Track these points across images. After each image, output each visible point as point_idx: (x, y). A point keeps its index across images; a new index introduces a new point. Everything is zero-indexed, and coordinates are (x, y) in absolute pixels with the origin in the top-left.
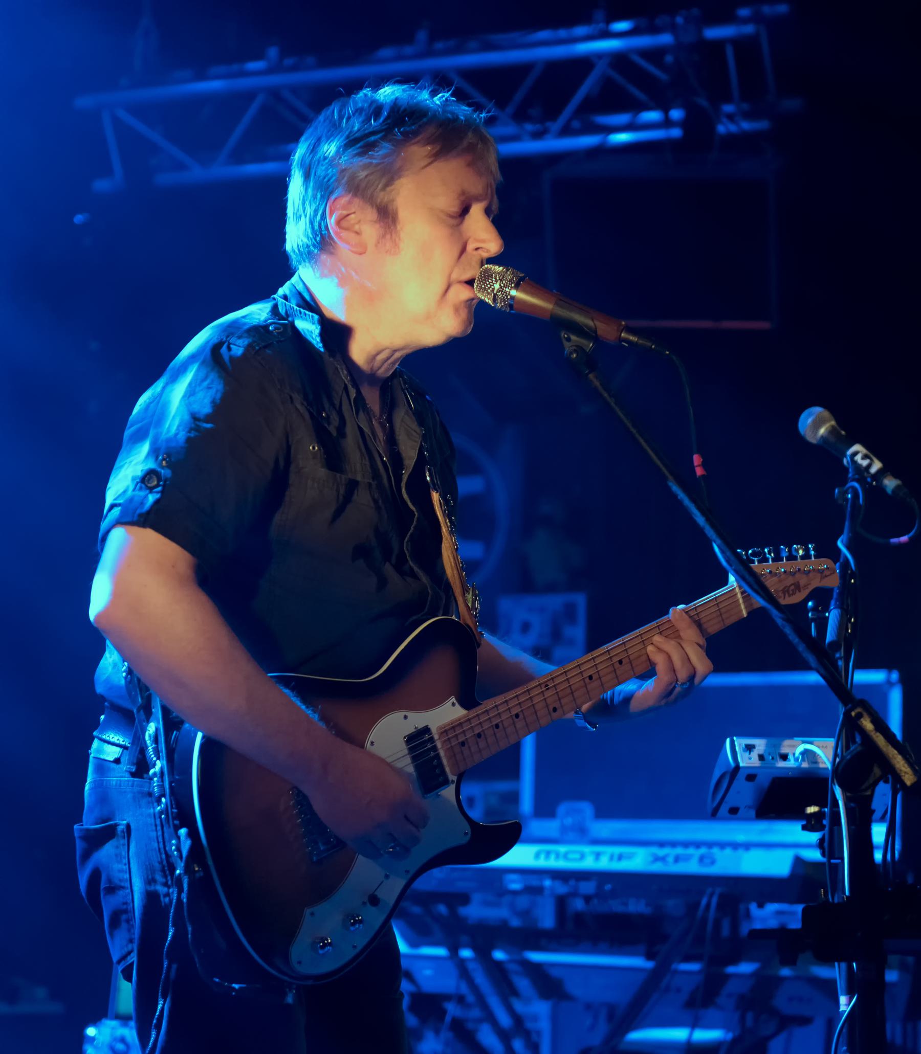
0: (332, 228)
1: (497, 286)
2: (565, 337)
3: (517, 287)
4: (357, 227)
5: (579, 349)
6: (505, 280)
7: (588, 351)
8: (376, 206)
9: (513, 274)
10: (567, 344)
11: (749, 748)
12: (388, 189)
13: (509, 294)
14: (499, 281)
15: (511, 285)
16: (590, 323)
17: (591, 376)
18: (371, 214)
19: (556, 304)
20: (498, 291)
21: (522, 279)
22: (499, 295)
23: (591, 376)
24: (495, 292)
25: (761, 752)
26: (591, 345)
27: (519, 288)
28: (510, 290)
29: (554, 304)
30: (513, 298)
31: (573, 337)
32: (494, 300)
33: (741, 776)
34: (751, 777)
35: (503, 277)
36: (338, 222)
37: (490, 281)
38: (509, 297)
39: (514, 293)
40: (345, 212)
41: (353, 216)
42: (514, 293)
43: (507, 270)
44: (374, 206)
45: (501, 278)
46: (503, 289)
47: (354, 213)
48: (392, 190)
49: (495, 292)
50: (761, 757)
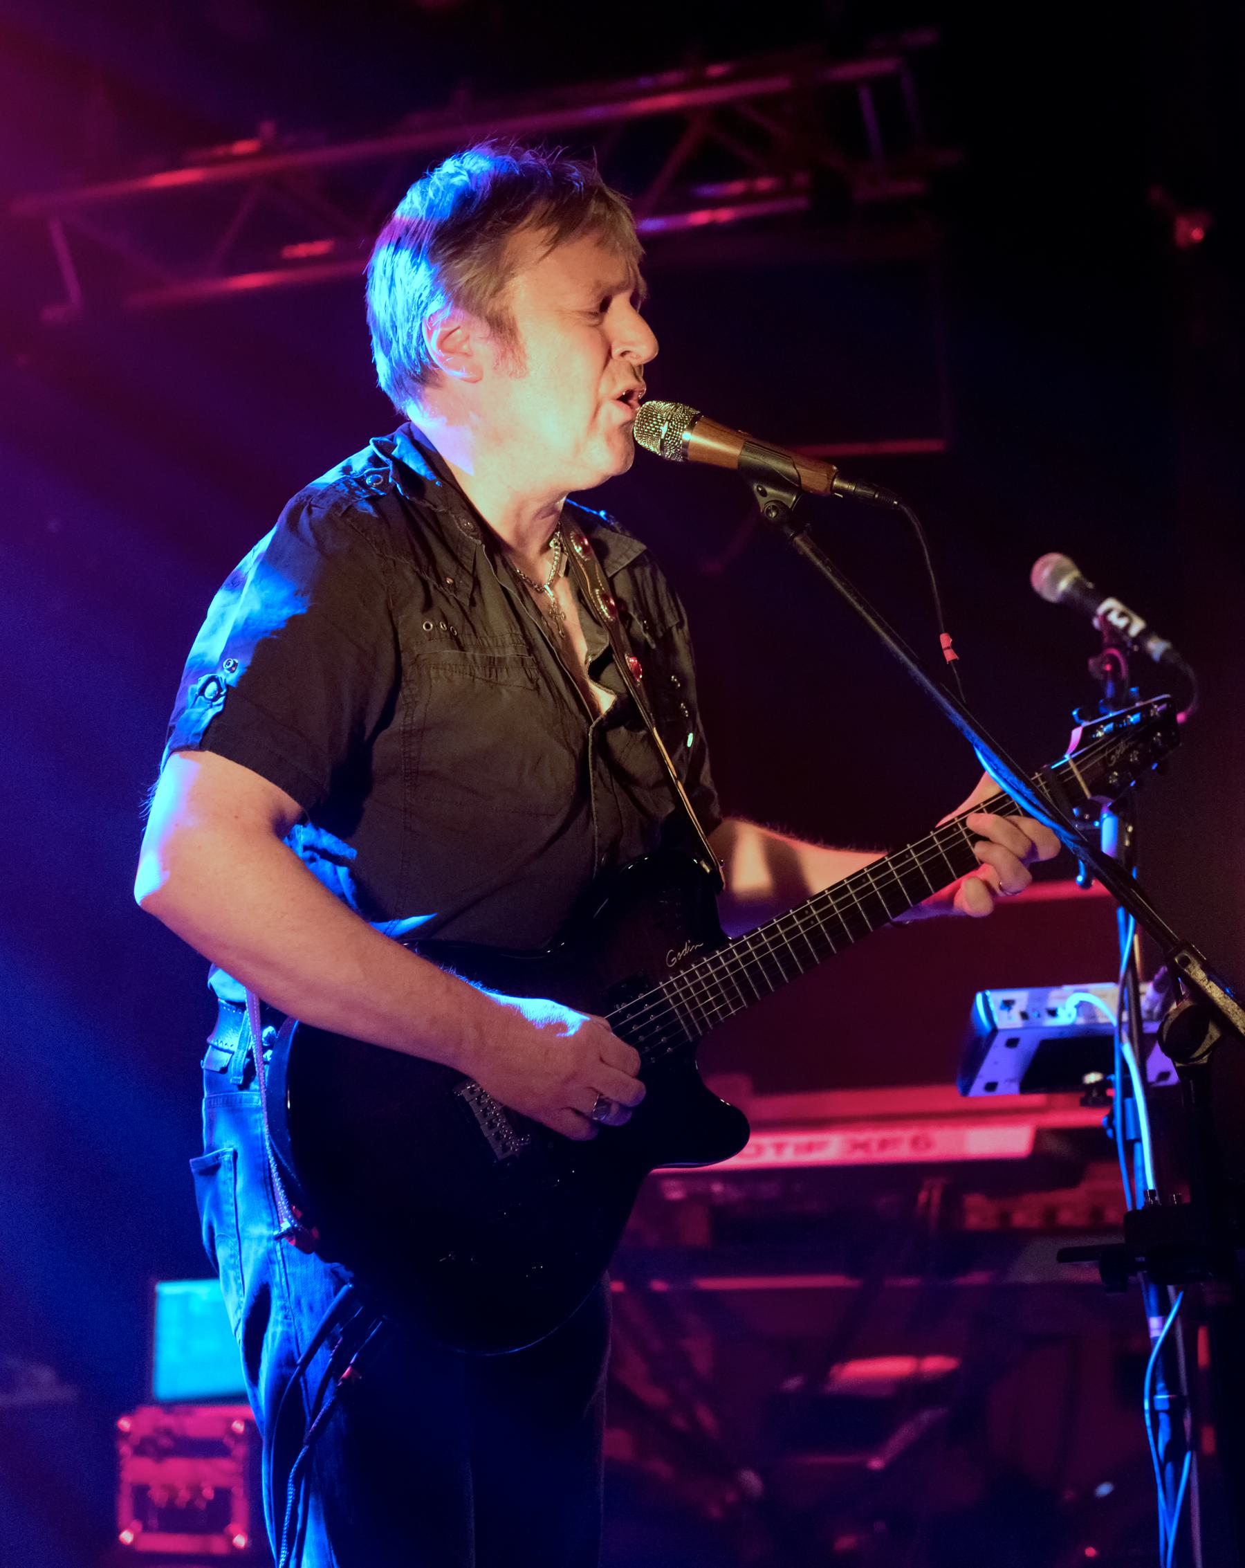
0: (434, 353)
1: (664, 429)
2: (758, 490)
3: (691, 427)
4: (465, 347)
5: (779, 505)
6: (674, 420)
7: (790, 507)
8: (486, 317)
9: (683, 412)
10: (762, 501)
11: (1008, 1004)
12: (499, 294)
13: (681, 439)
14: (667, 422)
15: (683, 426)
16: (791, 470)
17: (797, 539)
18: (481, 329)
19: (744, 447)
20: (667, 435)
21: (696, 418)
22: (669, 441)
23: (797, 539)
24: (663, 437)
25: (1023, 1008)
26: (794, 498)
27: (694, 430)
28: (682, 432)
29: (742, 449)
30: (686, 445)
31: (769, 490)
32: (662, 448)
33: (1000, 1040)
34: (1012, 1043)
35: (672, 417)
36: (441, 344)
37: (655, 423)
38: (681, 442)
39: (687, 436)
40: (447, 329)
41: (459, 331)
42: (687, 436)
43: (677, 407)
44: (483, 317)
45: (669, 418)
46: (673, 433)
47: (458, 328)
48: (504, 294)
49: (663, 437)
50: (1024, 1015)
